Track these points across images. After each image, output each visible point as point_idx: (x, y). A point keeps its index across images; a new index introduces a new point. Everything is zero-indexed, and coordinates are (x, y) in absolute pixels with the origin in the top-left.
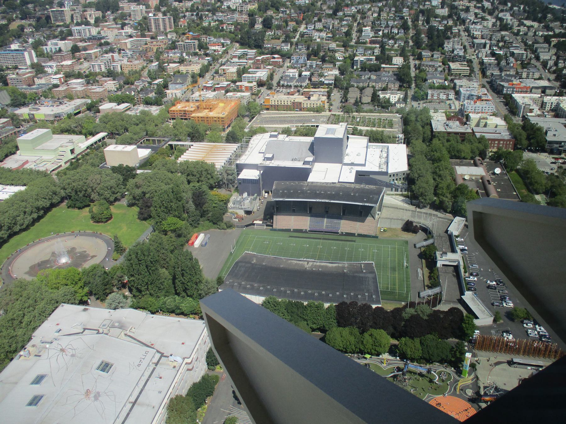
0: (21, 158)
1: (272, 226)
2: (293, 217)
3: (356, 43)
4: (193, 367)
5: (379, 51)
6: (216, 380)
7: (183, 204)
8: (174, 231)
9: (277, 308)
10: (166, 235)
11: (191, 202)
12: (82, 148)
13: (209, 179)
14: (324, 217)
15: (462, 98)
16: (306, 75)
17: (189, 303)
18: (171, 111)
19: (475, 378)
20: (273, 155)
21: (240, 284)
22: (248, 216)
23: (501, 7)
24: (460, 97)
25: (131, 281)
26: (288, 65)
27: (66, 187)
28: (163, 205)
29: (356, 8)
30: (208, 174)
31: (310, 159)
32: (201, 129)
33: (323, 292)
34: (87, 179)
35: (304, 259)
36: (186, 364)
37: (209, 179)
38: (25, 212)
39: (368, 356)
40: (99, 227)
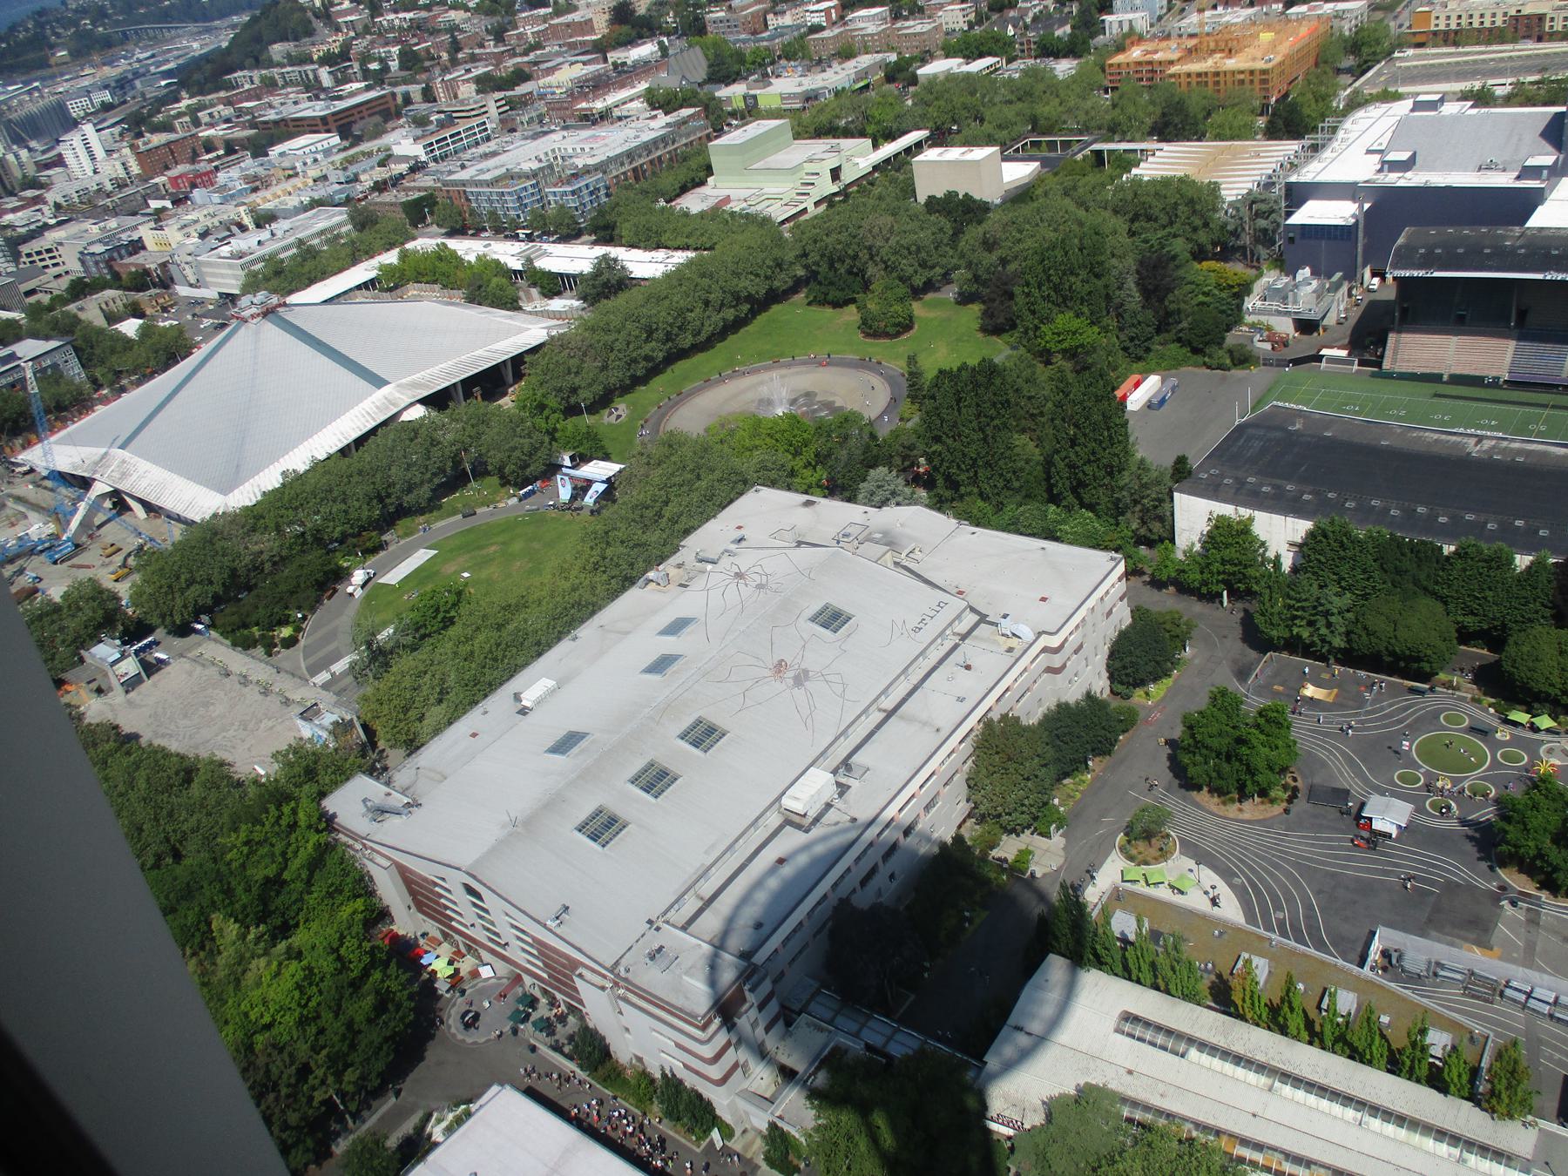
0: (716, 192)
1: (1379, 364)
2: (1455, 339)
4: (1064, 666)
6: (1128, 721)
7: (1106, 286)
8: (1071, 354)
9: (1349, 554)
10: (1048, 363)
11: (1131, 283)
12: (861, 166)
13: (1195, 229)
17: (1083, 525)
18: (1111, 65)
20: (1413, 157)
21: (1241, 483)
22: (1305, 337)
25: (934, 452)
27: (808, 248)
28: (1049, 280)
30: (1194, 212)
31: (1548, 159)
32: (1195, 104)
33: (1519, 523)
34: (860, 227)
35: (1469, 431)
36: (1045, 650)
37: (1195, 229)
38: (707, 303)
40: (878, 348)
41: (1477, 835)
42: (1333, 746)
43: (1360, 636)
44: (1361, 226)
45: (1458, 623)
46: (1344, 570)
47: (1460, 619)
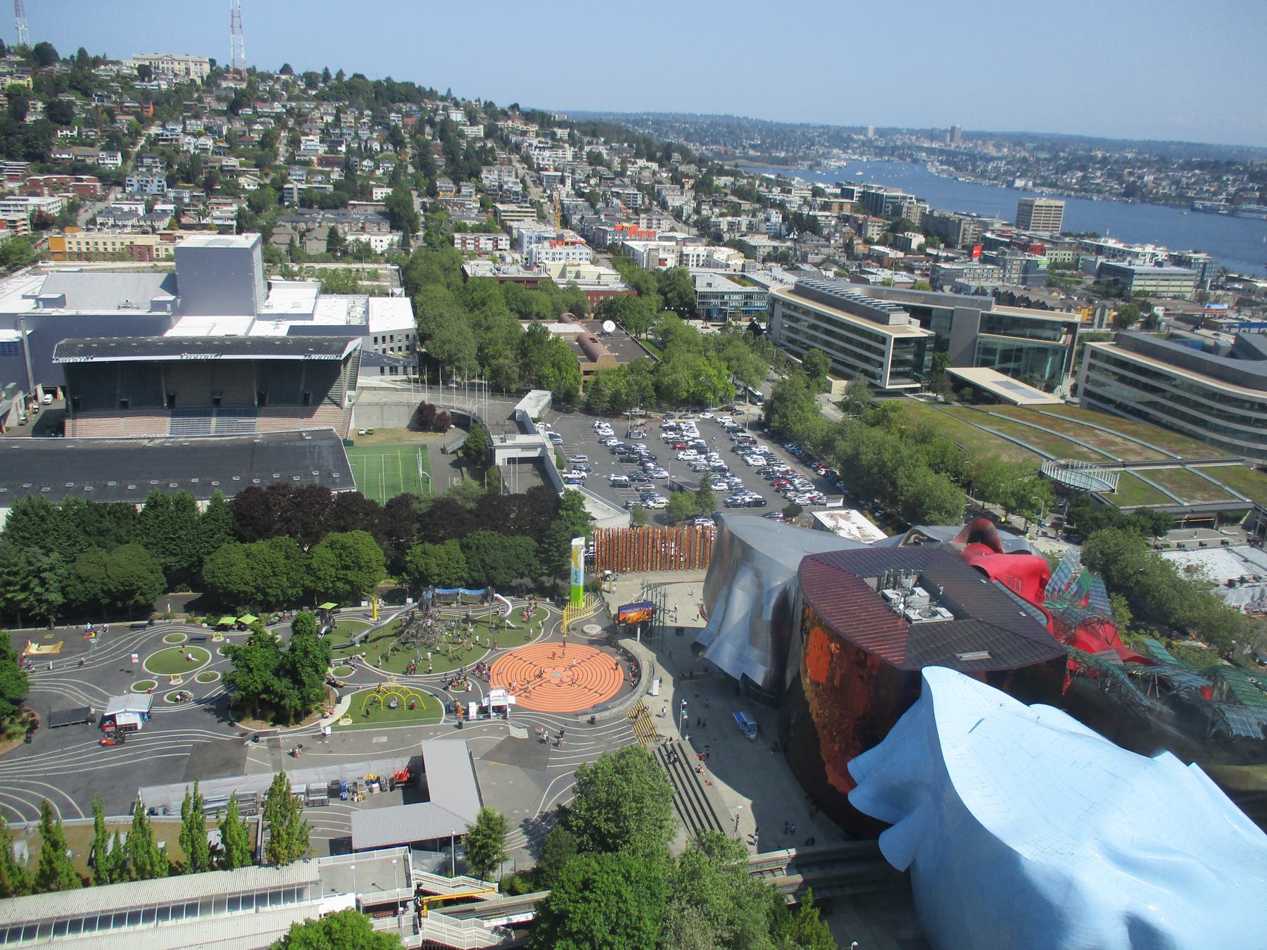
3: (291, 161)
5: (340, 176)
14: (209, 414)
15: (525, 244)
16: (163, 211)
19: (602, 606)
23: (586, 139)
24: (521, 246)
26: (119, 196)
29: (284, 106)
33: (193, 480)
39: (329, 606)
41: (214, 707)
42: (66, 682)
43: (74, 586)
44: (26, 345)
45: (162, 564)
46: (49, 541)
47: (163, 561)
